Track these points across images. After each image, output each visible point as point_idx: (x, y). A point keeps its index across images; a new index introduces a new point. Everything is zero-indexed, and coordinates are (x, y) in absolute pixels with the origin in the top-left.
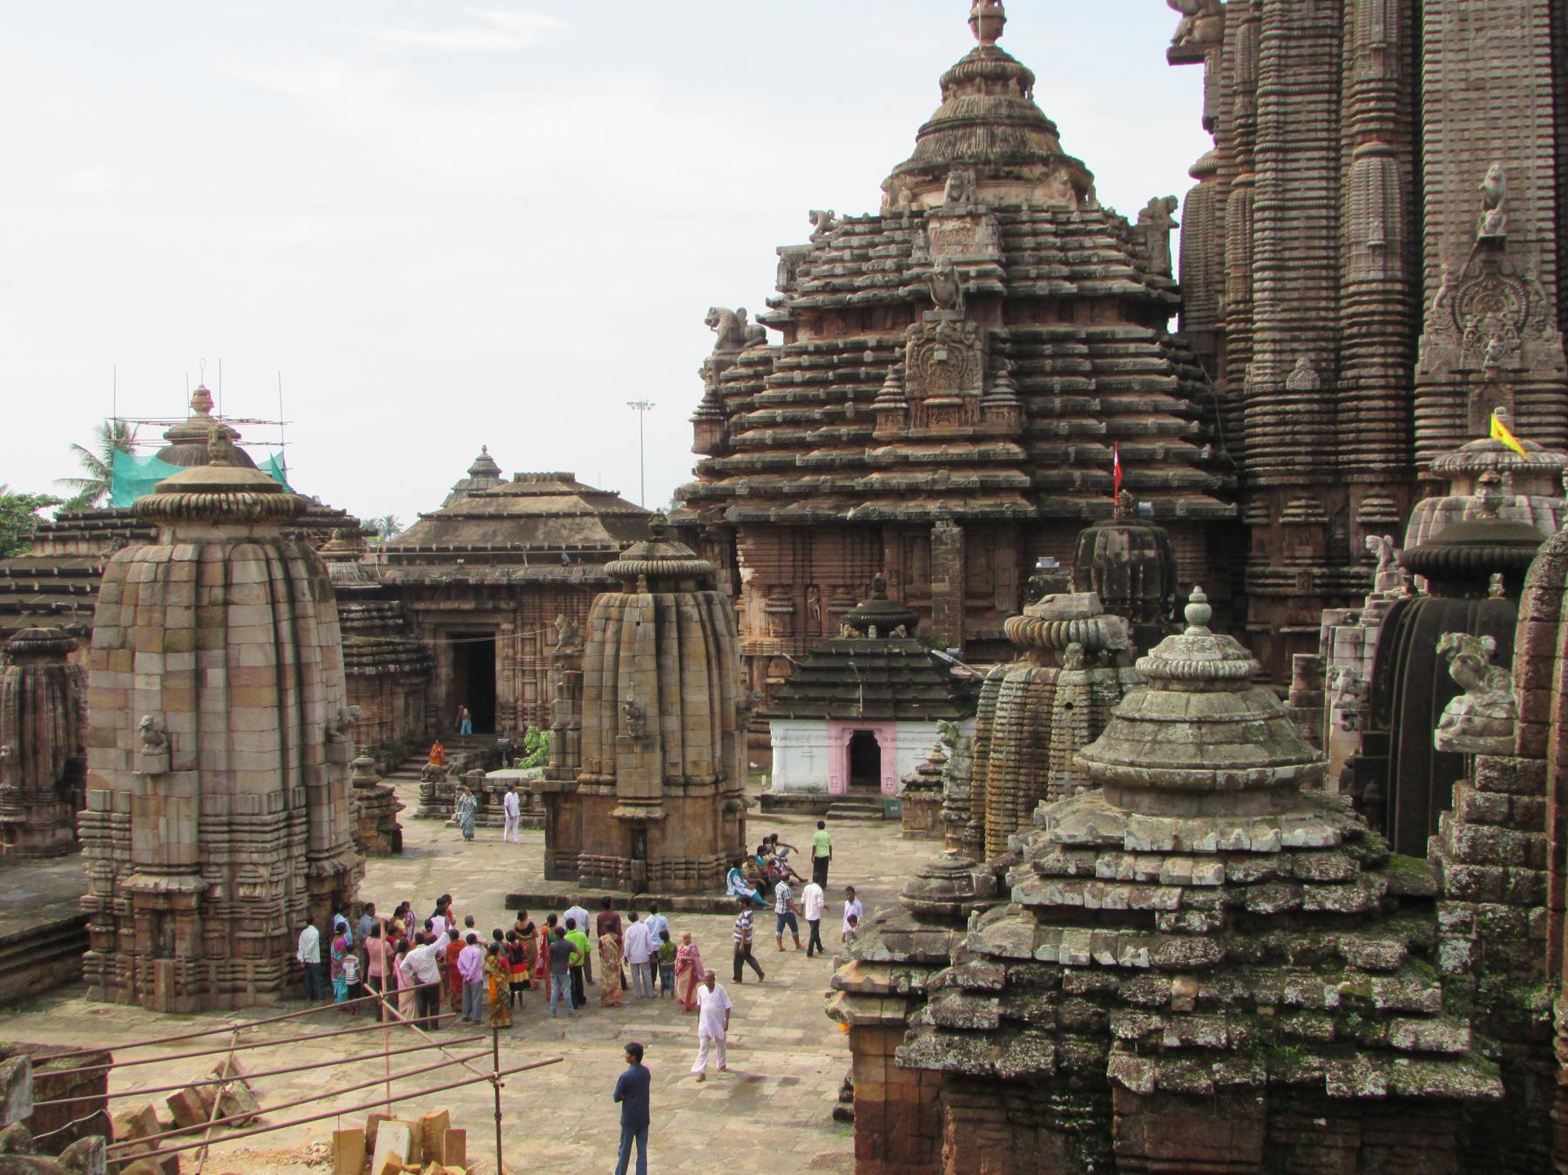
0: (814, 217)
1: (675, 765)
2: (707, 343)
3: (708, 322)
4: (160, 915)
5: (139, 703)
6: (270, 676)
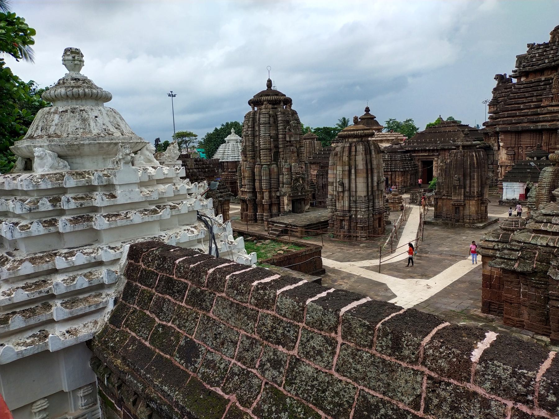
0: (529, 45)
1: (467, 192)
2: (495, 83)
3: (495, 78)
4: (342, 221)
5: (338, 177)
6: (365, 171)
